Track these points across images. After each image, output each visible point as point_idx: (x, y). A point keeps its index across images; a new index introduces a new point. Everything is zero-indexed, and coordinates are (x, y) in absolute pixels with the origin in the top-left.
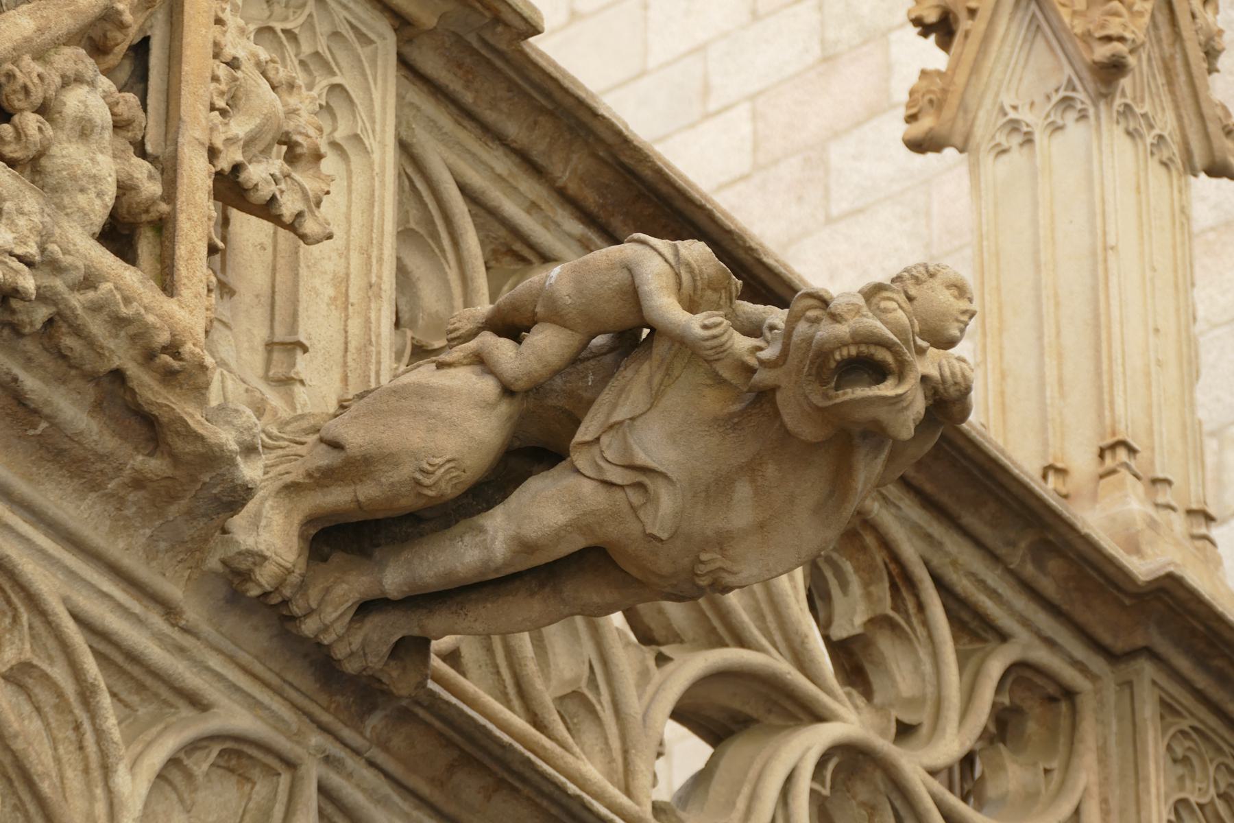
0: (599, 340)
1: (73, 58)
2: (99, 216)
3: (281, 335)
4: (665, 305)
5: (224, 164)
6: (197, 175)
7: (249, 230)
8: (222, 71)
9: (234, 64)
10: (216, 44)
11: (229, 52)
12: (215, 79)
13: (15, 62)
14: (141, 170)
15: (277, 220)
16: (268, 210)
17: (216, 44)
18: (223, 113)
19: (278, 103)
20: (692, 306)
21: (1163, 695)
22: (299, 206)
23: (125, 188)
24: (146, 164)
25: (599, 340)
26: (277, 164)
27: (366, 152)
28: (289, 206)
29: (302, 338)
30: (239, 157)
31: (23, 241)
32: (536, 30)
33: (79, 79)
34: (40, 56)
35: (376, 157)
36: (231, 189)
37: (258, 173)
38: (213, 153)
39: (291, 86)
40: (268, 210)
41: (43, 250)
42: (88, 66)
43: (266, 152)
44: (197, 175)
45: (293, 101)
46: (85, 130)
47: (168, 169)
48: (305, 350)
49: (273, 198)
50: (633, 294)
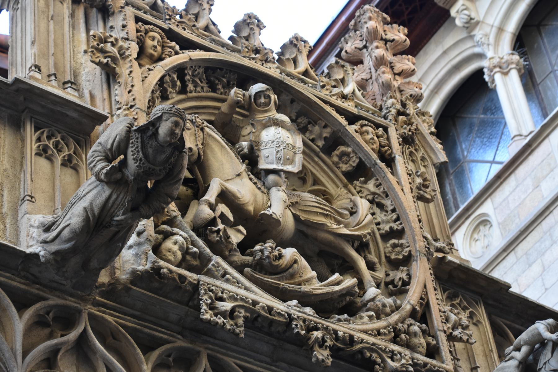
0: (537, 346)
1: (410, 321)
2: (424, 351)
3: (473, 366)
4: (547, 335)
5: (448, 333)
6: (442, 337)
7: (459, 346)
8: (442, 314)
9: (444, 312)
10: (439, 309)
11: (443, 310)
12: (441, 316)
13: (397, 325)
14: (430, 339)
15: (463, 341)
16: (460, 340)
17: (439, 309)
18: (445, 323)
19: (456, 318)
20: (552, 332)
21: (209, 352)
22: (467, 337)
23: (428, 344)
24: (431, 338)
25: (537, 346)
26: (460, 330)
27: (481, 323)
28: (465, 338)
29: (478, 365)
30: (451, 331)
31: (408, 361)
32: (510, 287)
33: (411, 324)
34: (403, 322)
35: (484, 323)
36: (451, 338)
37: (456, 333)
38: (445, 332)
39: (459, 313)
40: (460, 340)
41: (412, 361)
42: (412, 321)
43: (457, 328)
44: (442, 337)
45: (460, 316)
46: (415, 334)
47: (435, 337)
48: (479, 367)
49: (461, 337)
50: (539, 334)
